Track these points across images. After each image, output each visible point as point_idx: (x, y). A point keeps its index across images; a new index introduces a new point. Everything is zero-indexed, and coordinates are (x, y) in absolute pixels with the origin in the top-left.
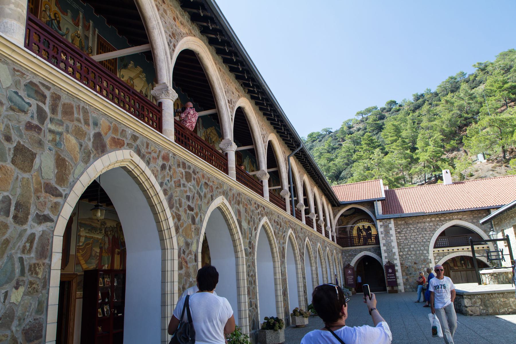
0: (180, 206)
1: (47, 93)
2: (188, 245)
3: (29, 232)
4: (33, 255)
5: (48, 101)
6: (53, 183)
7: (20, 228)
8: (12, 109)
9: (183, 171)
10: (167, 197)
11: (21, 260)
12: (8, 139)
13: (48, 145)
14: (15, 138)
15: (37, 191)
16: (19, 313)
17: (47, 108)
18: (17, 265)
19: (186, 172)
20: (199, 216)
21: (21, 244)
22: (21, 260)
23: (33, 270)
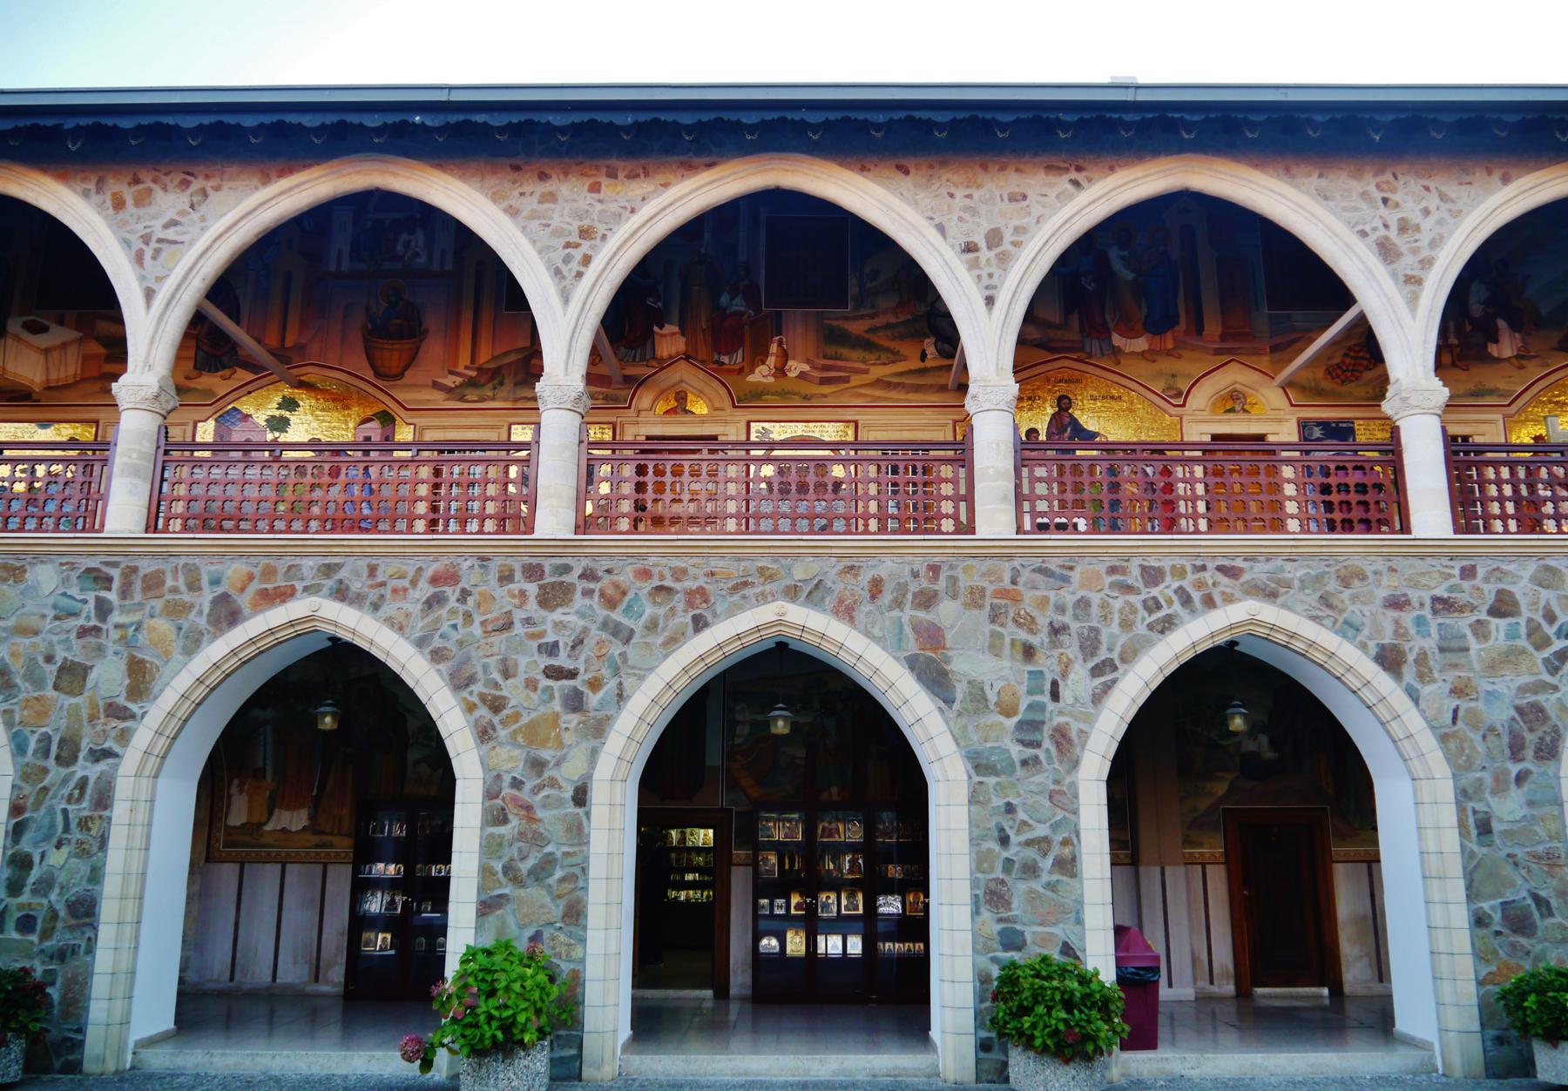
0: (507, 674)
1: (116, 573)
2: (537, 765)
3: (79, 774)
4: (85, 804)
5: (116, 585)
6: (121, 701)
7: (64, 771)
8: (57, 618)
9: (532, 589)
10: (442, 666)
11: (65, 812)
12: (49, 659)
13: (111, 648)
14: (60, 654)
15: (92, 718)
16: (62, 878)
17: (112, 596)
18: (59, 818)
19: (541, 587)
20: (610, 686)
21: (66, 791)
22: (65, 812)
23: (84, 824)
